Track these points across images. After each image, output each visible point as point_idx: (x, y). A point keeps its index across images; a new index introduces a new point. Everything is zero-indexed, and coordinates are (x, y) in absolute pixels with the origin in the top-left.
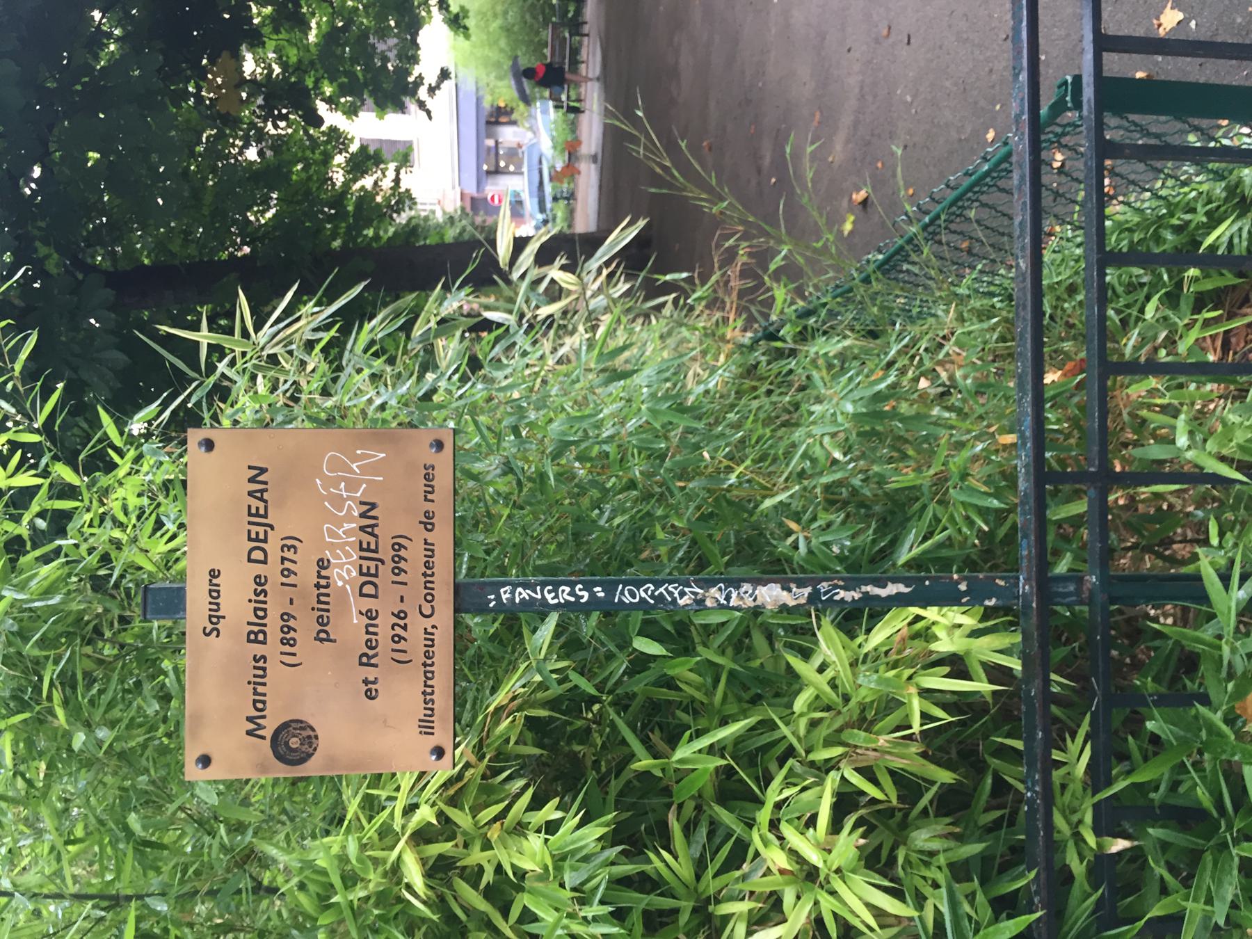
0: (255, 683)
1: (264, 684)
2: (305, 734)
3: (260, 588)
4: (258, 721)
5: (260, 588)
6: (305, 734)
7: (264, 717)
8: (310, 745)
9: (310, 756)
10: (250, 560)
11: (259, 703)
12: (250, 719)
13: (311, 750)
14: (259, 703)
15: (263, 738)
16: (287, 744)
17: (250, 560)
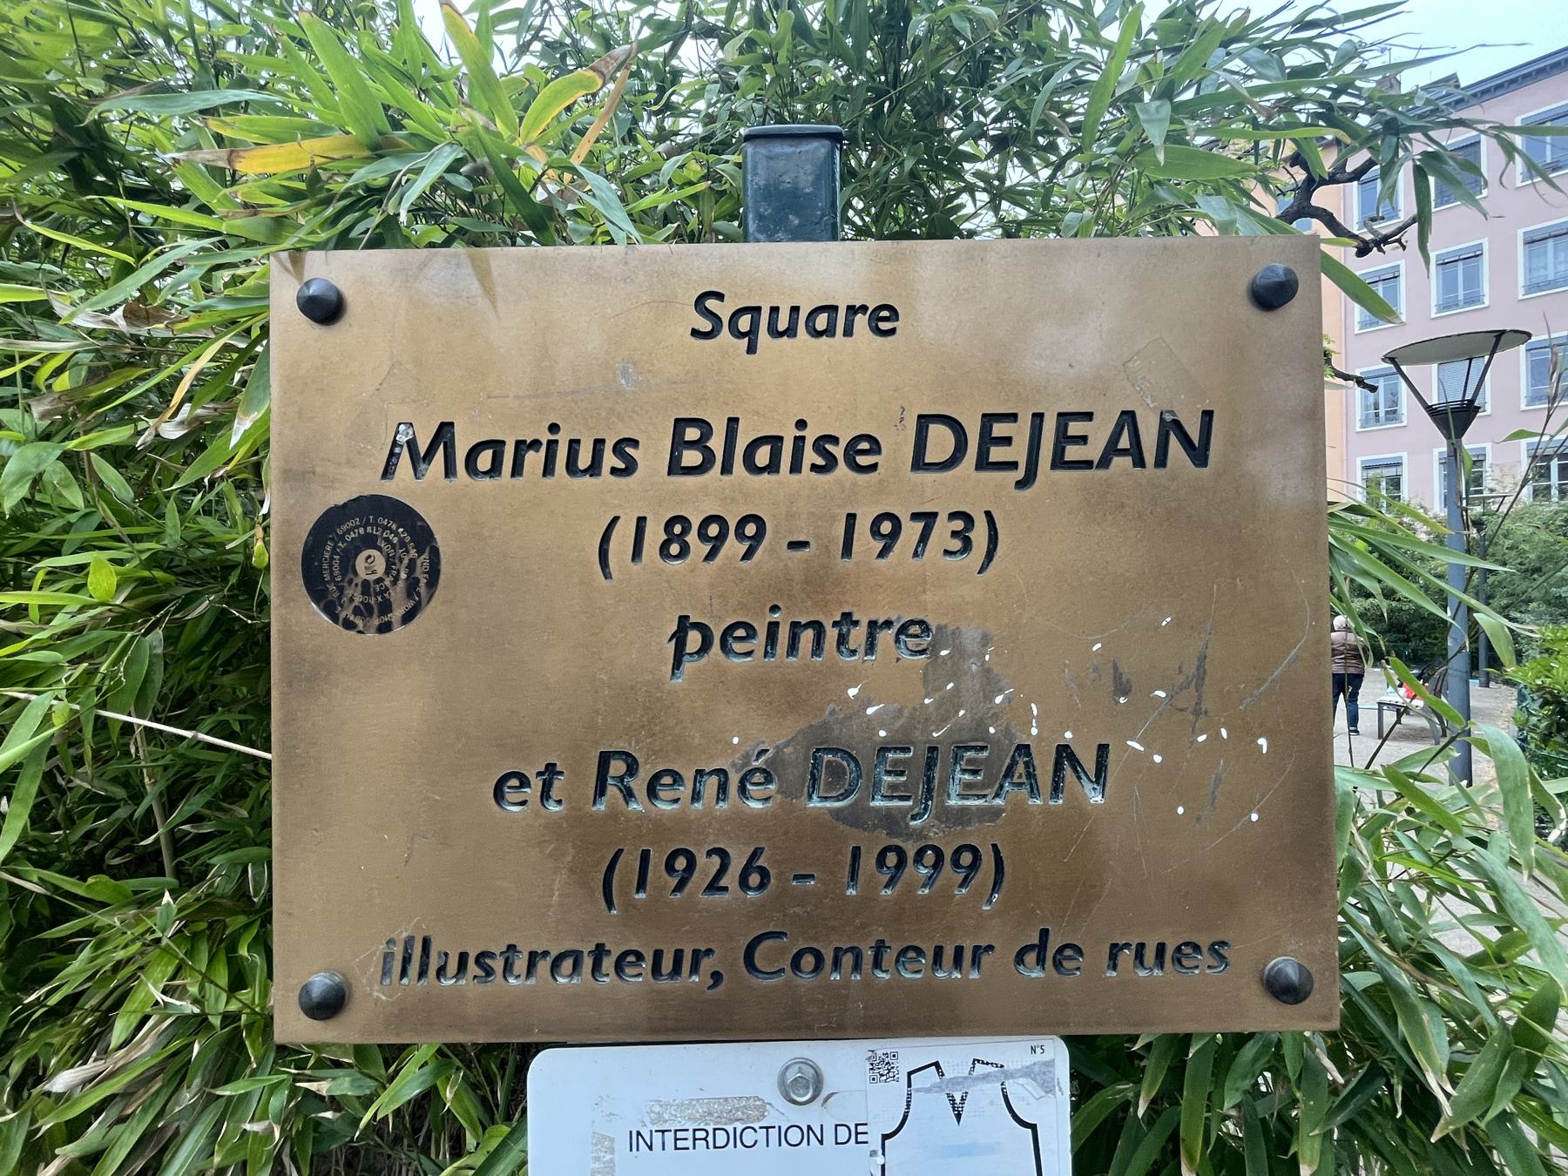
0: (552, 444)
1: (548, 470)
2: (397, 595)
3: (838, 451)
4: (440, 454)
5: (838, 451)
6: (397, 595)
7: (450, 471)
8: (364, 611)
9: (331, 611)
10: (924, 421)
11: (495, 457)
12: (444, 433)
13: (347, 613)
14: (495, 457)
15: (388, 472)
16: (370, 542)
17: (924, 421)
